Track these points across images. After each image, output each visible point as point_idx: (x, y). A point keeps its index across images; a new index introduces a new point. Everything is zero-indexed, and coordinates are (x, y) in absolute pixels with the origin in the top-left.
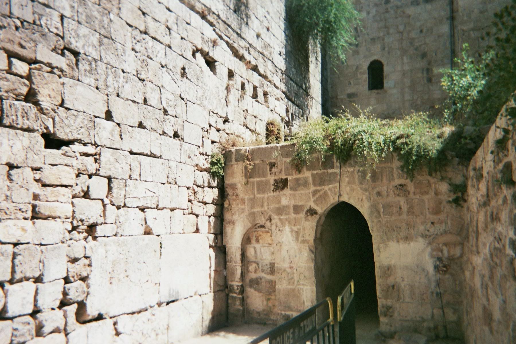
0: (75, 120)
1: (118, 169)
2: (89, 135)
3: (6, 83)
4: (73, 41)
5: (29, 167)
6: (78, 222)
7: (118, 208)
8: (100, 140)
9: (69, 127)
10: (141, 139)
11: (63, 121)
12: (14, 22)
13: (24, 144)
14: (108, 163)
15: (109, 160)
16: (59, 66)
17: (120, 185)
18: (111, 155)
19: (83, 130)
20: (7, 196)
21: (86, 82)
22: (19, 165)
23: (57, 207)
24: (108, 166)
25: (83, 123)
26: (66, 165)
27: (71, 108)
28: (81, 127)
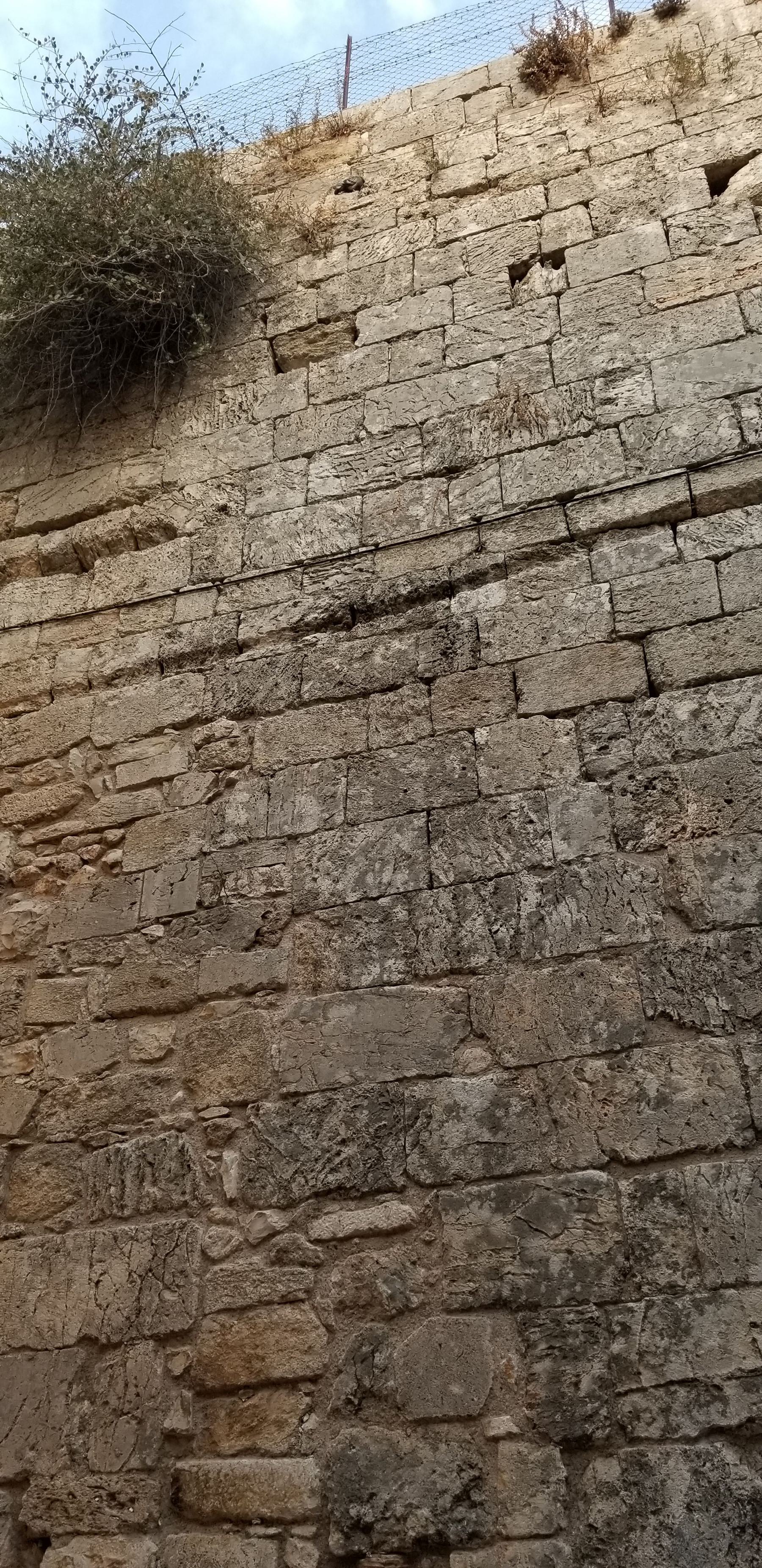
0: (320, 1124)
1: (544, 1262)
2: (380, 1158)
3: (104, 1102)
4: (325, 885)
5: (145, 1338)
6: (347, 1537)
7: (577, 1447)
8: (433, 1166)
9: (293, 1157)
10: (677, 1090)
11: (270, 1146)
12: (145, 934)
13: (134, 1266)
14: (484, 1245)
15: (486, 1236)
16: (265, 980)
17: (564, 1335)
18: (496, 1210)
19: (348, 1151)
20: (72, 1452)
21: (366, 980)
22: (115, 1339)
23: (246, 1477)
24: (484, 1261)
25: (348, 1123)
26: (288, 1300)
27: (302, 1089)
28: (343, 1142)
